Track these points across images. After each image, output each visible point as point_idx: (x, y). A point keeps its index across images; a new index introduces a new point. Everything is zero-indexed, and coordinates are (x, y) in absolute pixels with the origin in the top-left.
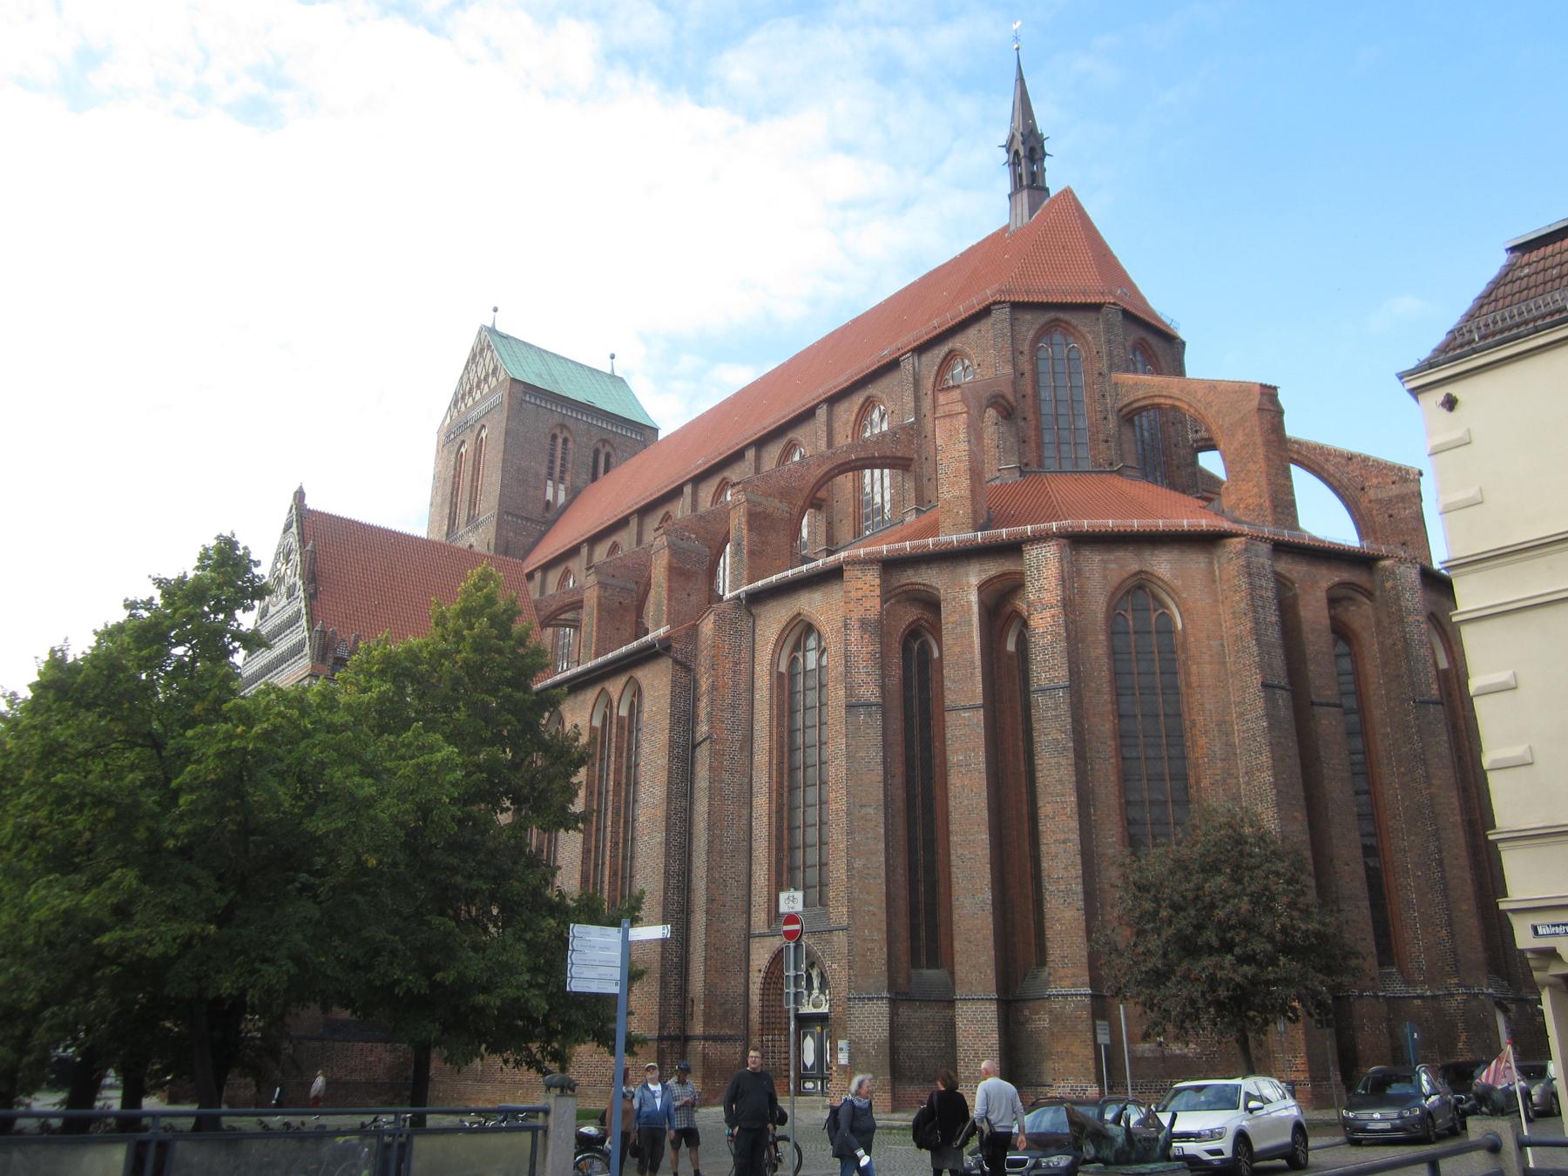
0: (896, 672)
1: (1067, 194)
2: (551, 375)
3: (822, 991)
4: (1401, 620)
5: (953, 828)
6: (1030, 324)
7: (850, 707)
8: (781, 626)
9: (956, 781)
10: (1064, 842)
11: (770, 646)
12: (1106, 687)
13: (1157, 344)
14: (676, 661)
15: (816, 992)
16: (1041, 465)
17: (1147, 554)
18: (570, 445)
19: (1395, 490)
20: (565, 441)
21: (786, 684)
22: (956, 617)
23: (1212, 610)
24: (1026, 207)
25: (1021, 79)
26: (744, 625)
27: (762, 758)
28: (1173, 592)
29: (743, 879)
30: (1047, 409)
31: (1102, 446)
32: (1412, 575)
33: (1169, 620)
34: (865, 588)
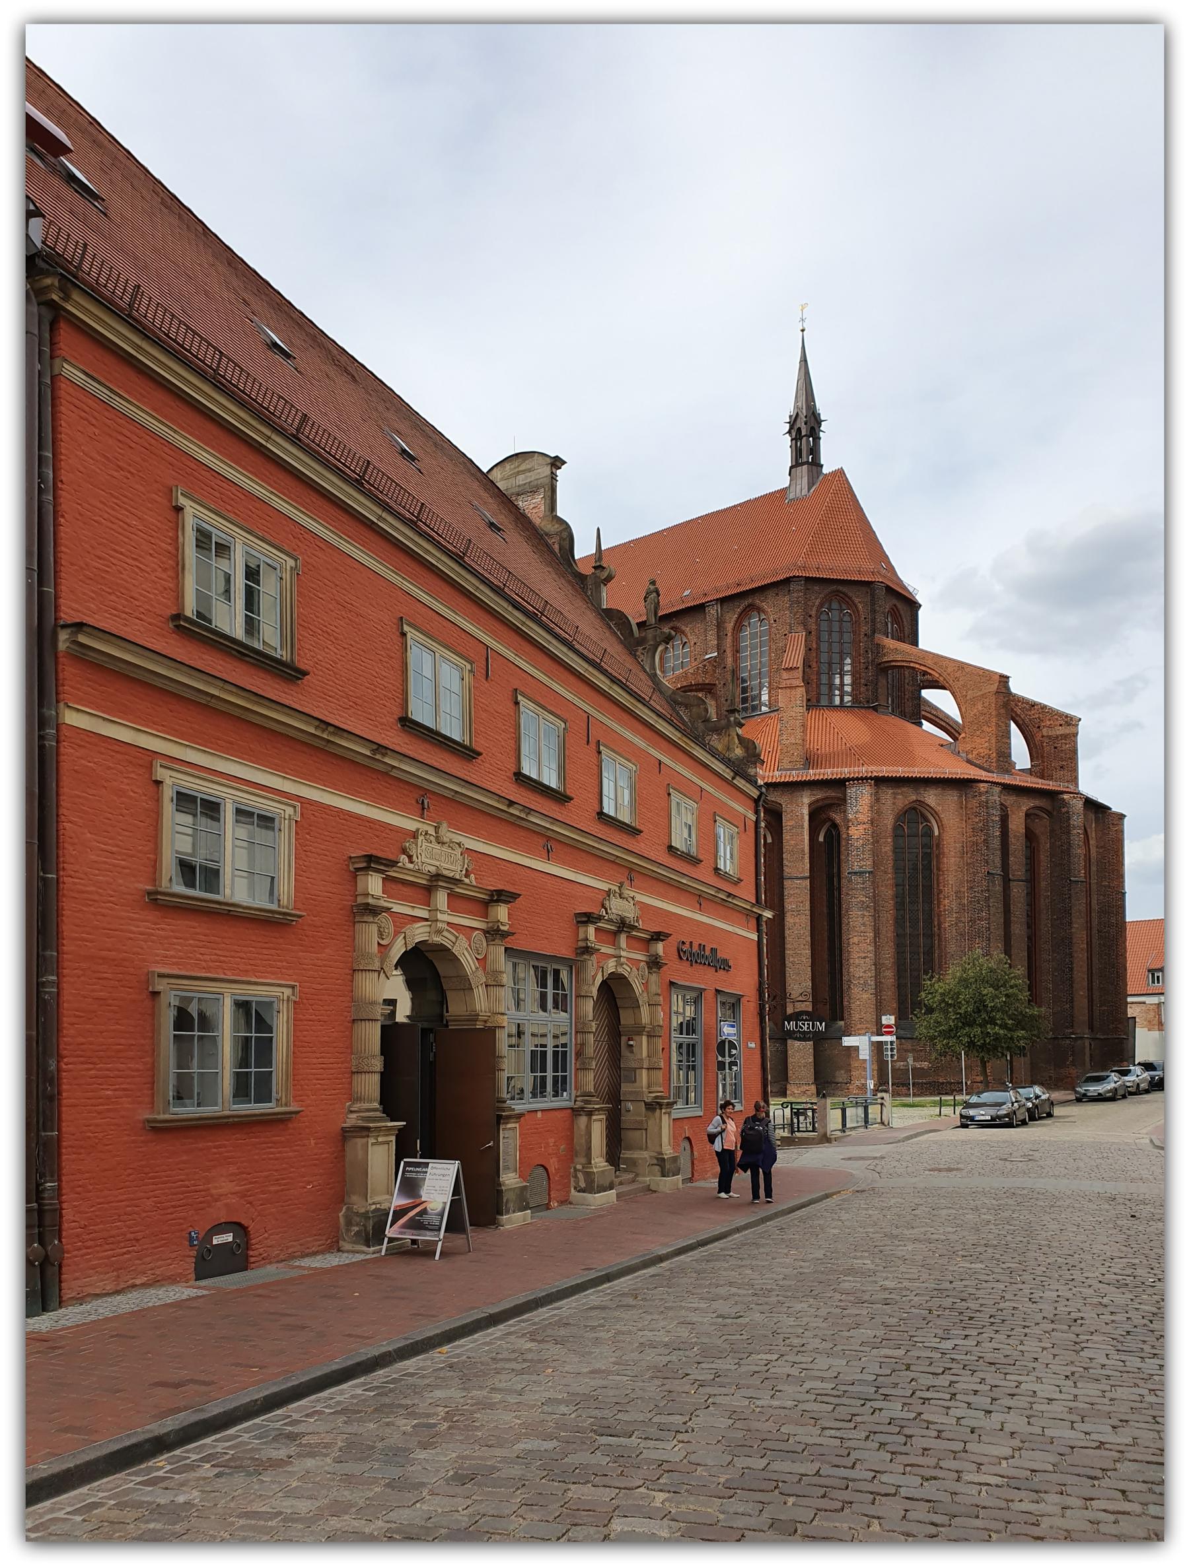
1: (840, 473)
4: (1069, 833)
13: (903, 609)
16: (818, 701)
22: (792, 823)
23: (950, 820)
24: (805, 480)
25: (804, 360)
30: (824, 658)
31: (863, 689)
32: (1079, 805)
33: (931, 829)
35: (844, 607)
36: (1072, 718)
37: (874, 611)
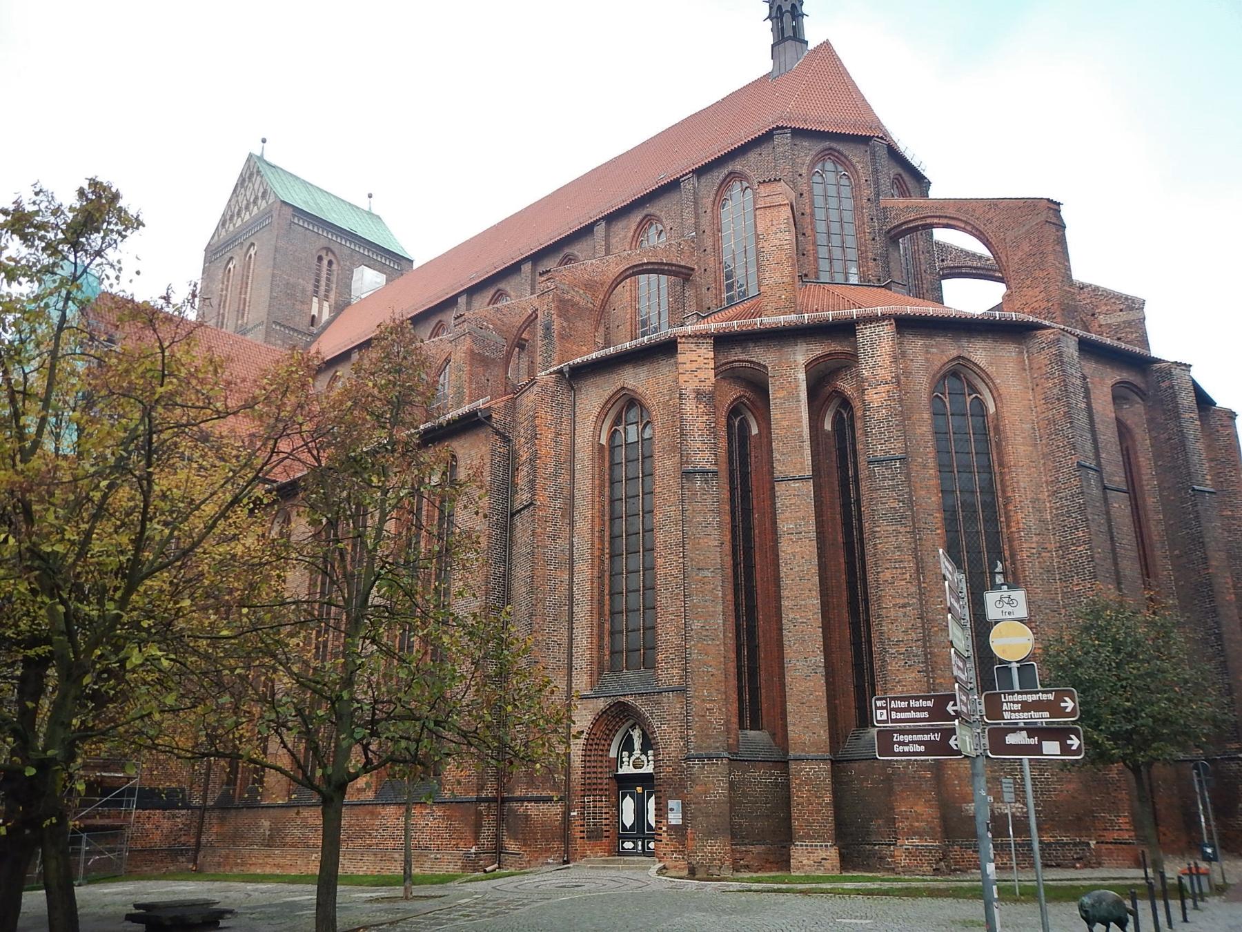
0: (723, 444)
1: (826, 45)
2: (317, 204)
3: (644, 751)
5: (784, 593)
6: (807, 151)
7: (687, 475)
8: (603, 400)
9: (786, 548)
10: (904, 606)
11: (592, 419)
12: (931, 463)
13: (911, 178)
14: (497, 432)
15: (637, 753)
17: (964, 342)
18: (335, 267)
19: (1124, 316)
20: (330, 263)
21: (608, 454)
26: (565, 398)
27: (584, 526)
28: (986, 378)
29: (565, 641)
31: (871, 264)
34: (697, 366)
35: (840, 168)
36: (1133, 300)
37: (875, 171)
